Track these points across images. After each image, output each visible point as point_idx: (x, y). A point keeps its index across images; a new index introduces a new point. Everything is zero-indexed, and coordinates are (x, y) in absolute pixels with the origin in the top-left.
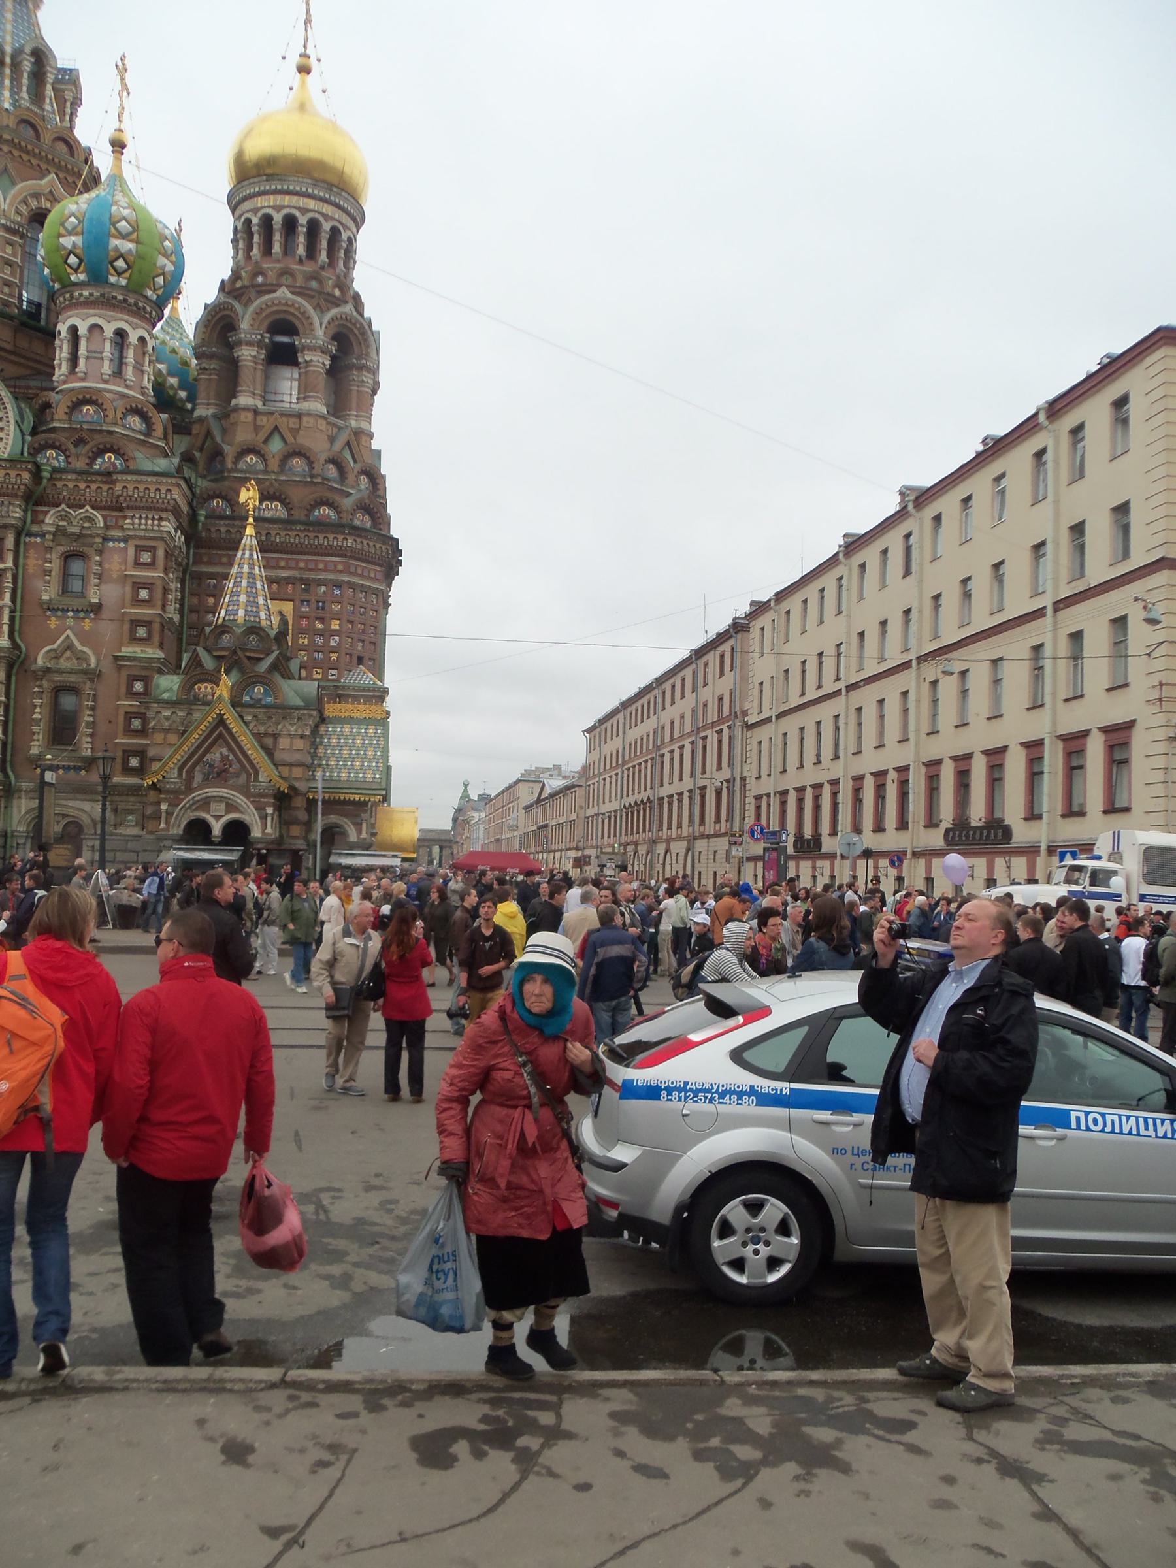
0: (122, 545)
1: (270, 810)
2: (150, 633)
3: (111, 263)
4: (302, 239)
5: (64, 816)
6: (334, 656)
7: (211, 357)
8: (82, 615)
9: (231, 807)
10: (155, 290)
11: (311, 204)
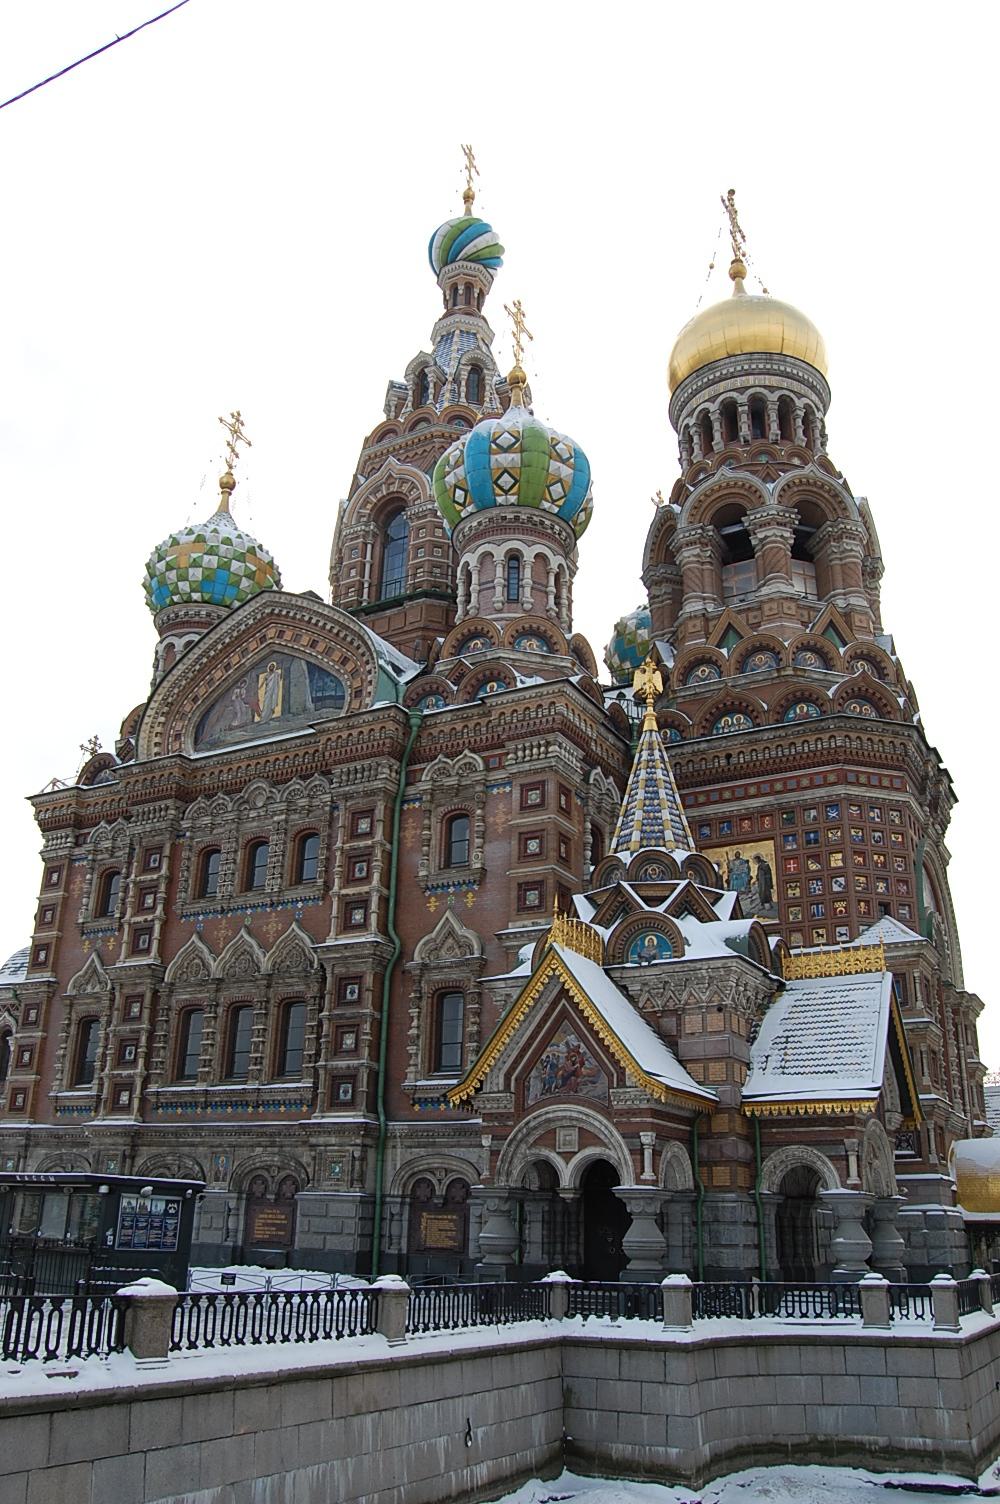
0: (508, 789)
1: (647, 1138)
2: (541, 897)
3: (496, 483)
4: (744, 418)
5: (446, 1170)
6: (840, 906)
7: (657, 583)
8: (464, 888)
9: (587, 1137)
10: (553, 502)
11: (751, 380)
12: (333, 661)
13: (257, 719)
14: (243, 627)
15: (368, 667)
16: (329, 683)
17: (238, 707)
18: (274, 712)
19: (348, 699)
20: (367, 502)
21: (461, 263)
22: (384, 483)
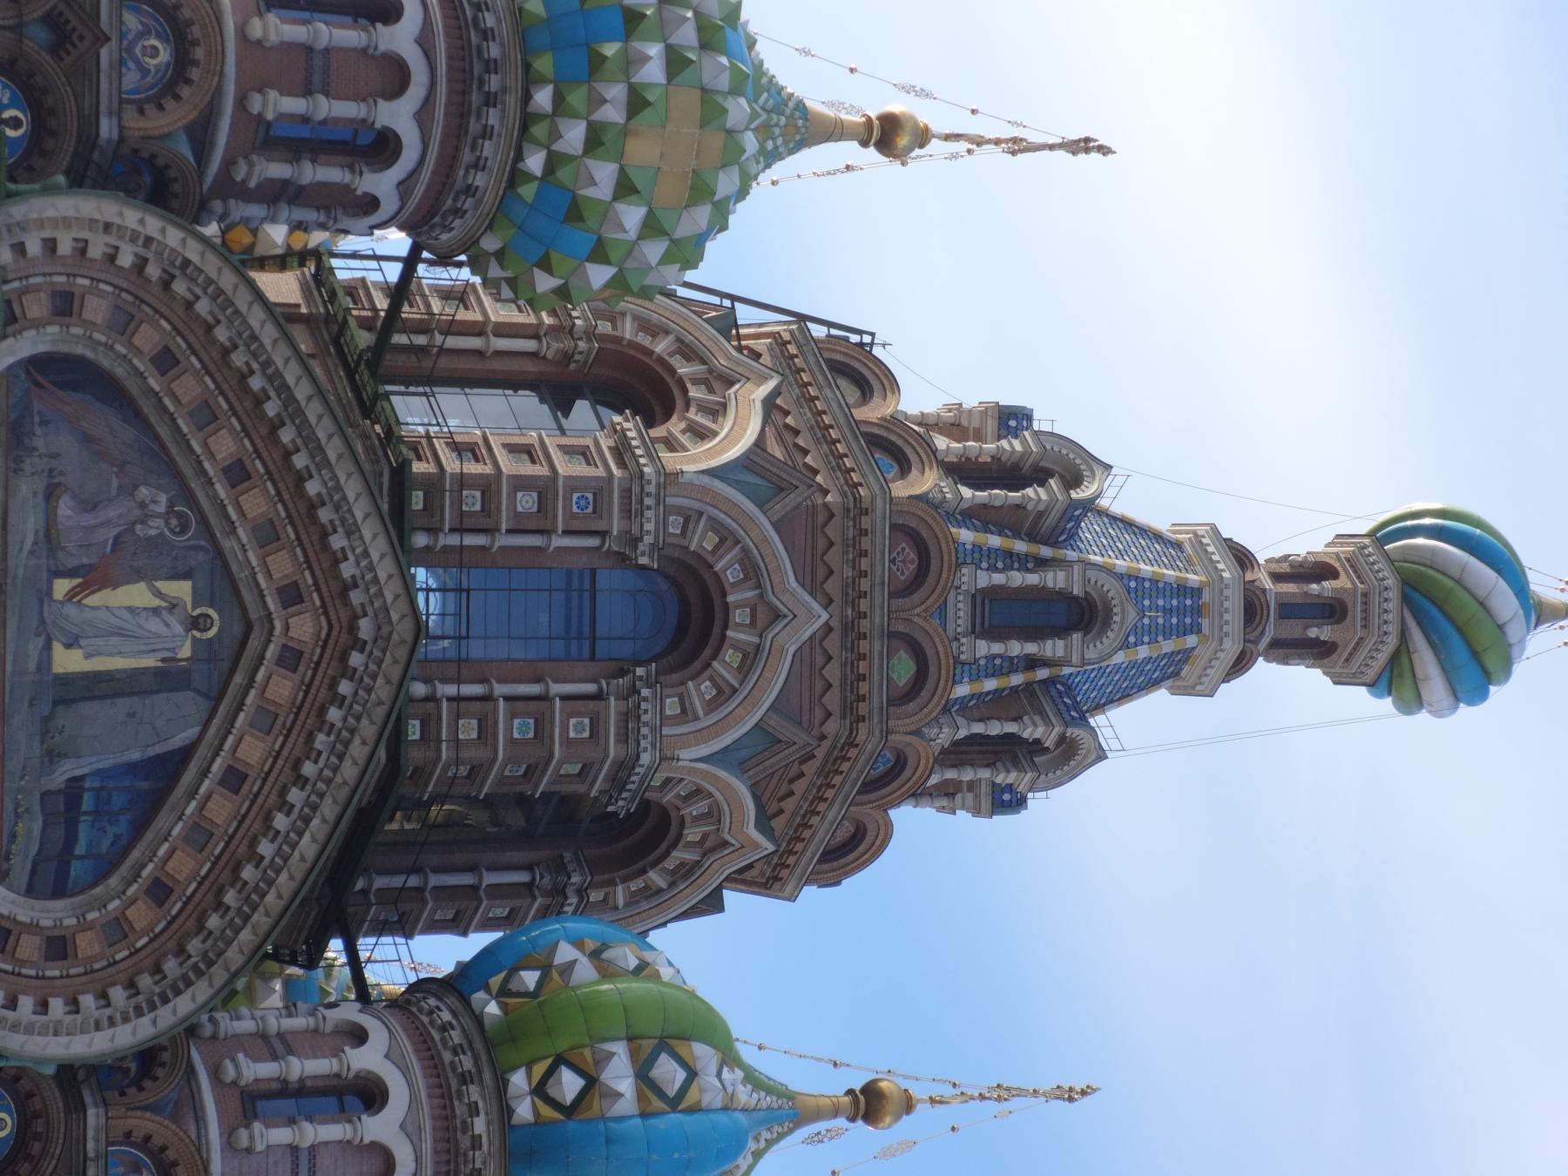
12: (170, 854)
13: (62, 587)
14: (337, 542)
15: (118, 994)
16: (112, 830)
17: (111, 513)
18: (68, 646)
19: (54, 913)
20: (726, 538)
21: (1392, 642)
22: (761, 596)
